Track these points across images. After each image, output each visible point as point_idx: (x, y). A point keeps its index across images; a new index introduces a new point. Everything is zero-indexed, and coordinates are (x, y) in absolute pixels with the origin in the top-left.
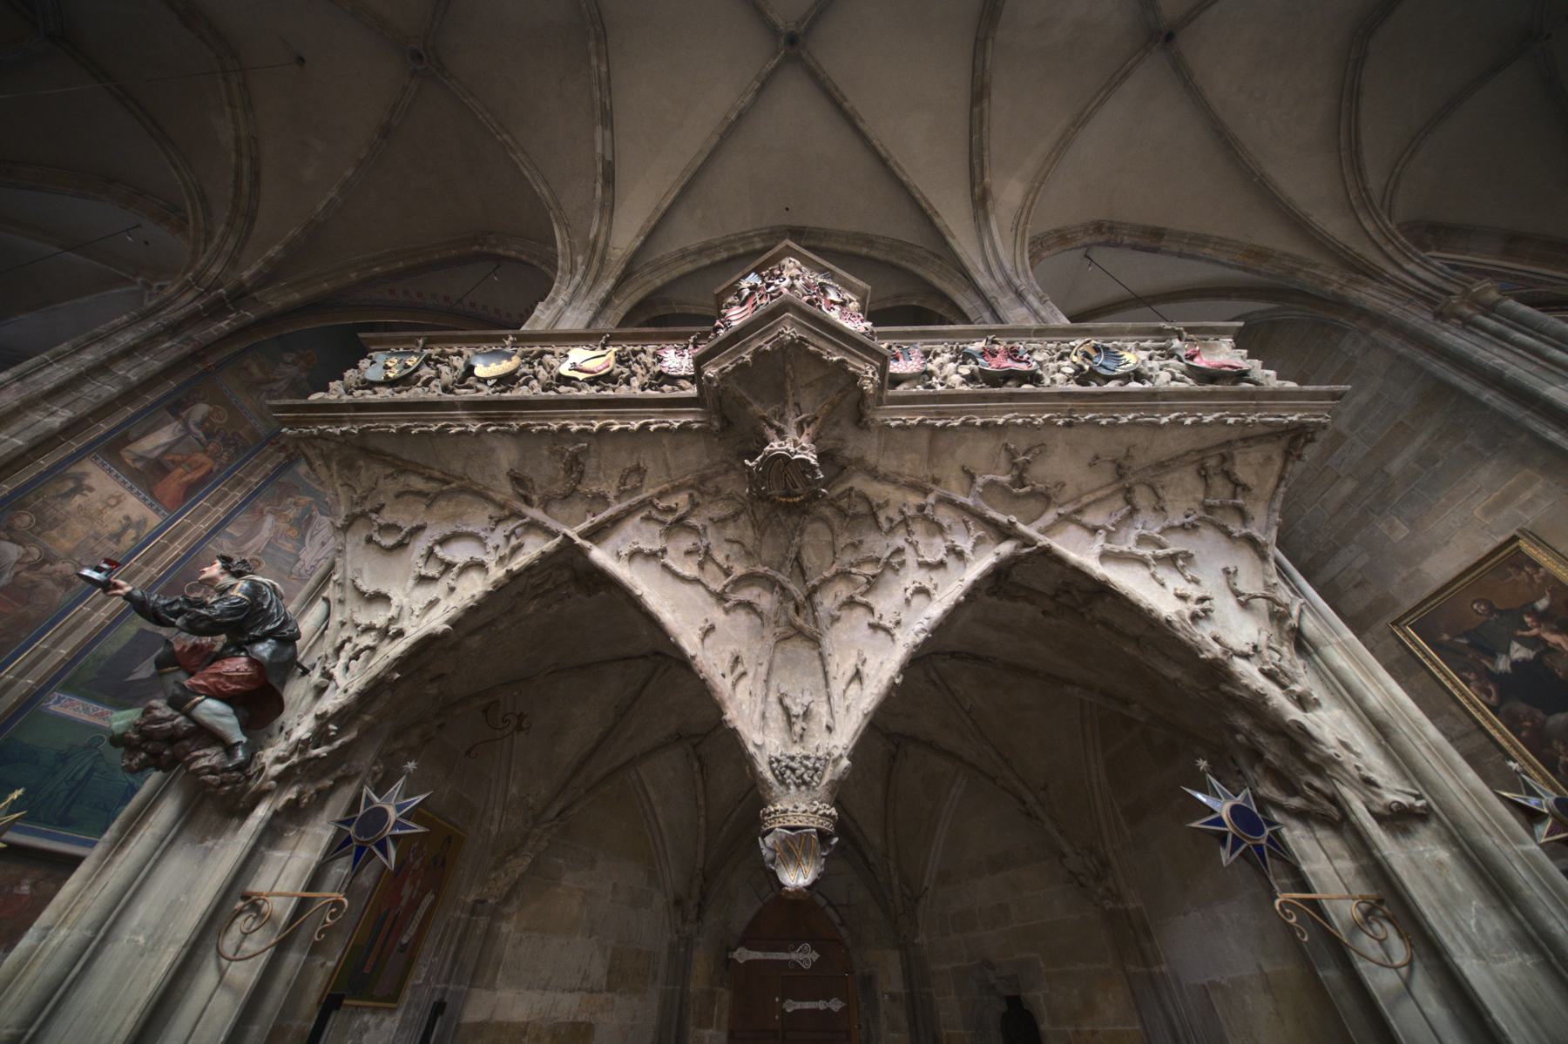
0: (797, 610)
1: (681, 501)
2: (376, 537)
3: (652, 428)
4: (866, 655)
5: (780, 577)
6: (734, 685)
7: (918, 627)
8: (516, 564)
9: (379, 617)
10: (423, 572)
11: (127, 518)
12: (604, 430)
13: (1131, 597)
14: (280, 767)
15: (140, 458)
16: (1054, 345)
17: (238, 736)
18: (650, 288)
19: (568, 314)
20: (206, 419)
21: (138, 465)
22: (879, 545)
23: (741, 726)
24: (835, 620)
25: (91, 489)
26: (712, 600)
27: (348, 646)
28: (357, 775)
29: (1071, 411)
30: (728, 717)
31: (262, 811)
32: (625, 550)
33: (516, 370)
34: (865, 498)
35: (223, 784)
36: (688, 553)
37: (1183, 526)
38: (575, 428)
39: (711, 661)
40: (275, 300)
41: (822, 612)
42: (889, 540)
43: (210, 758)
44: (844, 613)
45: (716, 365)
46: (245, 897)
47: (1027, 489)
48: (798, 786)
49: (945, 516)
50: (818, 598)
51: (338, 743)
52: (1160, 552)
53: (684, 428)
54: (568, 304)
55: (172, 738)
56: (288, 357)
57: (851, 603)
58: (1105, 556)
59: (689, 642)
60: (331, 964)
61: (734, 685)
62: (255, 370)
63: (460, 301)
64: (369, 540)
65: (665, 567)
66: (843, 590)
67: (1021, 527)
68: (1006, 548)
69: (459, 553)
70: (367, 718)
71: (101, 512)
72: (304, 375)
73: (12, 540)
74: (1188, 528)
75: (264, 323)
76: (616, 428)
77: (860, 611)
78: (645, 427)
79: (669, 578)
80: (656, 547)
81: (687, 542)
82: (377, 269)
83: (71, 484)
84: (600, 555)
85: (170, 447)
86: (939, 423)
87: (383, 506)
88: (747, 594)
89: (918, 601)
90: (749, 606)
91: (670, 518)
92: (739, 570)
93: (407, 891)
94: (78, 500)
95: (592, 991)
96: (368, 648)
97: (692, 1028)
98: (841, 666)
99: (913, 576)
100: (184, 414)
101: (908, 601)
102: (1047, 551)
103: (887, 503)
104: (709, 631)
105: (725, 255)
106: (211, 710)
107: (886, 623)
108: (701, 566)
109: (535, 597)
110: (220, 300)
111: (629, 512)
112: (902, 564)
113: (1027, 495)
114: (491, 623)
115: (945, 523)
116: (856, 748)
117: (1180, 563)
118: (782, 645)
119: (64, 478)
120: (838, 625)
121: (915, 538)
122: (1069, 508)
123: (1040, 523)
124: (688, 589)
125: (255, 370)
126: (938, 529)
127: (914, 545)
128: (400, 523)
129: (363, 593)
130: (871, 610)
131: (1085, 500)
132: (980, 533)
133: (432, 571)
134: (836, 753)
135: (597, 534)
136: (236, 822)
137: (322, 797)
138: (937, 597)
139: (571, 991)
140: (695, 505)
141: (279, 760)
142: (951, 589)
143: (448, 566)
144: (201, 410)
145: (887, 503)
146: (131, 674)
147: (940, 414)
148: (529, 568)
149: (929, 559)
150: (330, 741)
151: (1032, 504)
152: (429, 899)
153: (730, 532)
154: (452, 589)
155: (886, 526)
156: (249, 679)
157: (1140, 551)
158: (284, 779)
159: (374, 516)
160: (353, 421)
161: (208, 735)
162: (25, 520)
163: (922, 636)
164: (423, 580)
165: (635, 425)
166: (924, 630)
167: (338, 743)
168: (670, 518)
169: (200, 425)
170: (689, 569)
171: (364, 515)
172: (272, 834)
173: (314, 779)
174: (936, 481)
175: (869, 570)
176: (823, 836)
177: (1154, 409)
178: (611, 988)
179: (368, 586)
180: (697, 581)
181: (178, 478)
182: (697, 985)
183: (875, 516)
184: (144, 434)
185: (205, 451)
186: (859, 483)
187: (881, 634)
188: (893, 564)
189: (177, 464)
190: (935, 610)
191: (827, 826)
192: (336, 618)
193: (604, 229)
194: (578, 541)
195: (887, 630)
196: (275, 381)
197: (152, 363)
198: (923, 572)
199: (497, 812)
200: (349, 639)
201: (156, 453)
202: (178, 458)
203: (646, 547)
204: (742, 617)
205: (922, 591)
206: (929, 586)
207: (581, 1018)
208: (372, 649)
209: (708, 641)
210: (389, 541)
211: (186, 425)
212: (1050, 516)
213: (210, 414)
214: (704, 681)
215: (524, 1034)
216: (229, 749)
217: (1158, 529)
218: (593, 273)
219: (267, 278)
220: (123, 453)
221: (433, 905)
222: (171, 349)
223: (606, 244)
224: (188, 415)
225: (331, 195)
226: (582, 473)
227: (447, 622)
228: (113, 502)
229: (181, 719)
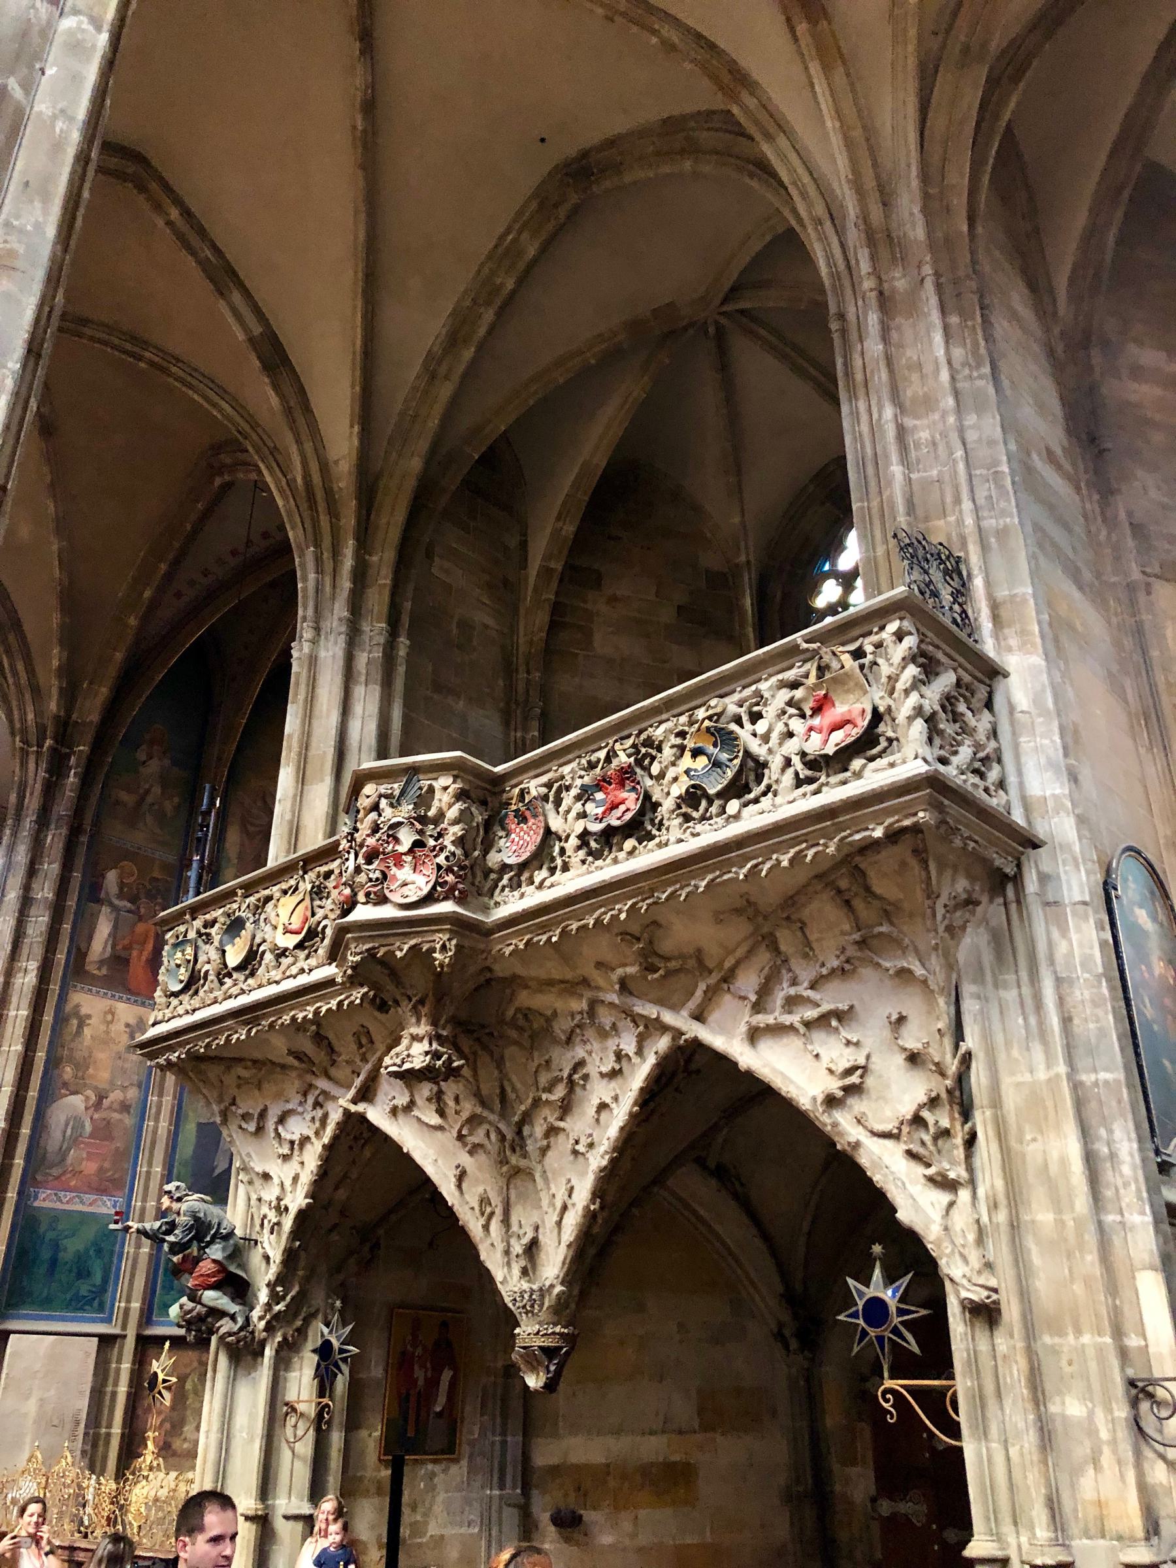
2: (244, 1126)
4: (573, 1182)
6: (486, 1227)
7: (602, 1149)
8: (326, 1140)
9: (270, 1193)
10: (281, 1151)
11: (127, 1025)
13: (773, 1085)
14: (262, 1324)
15: (102, 962)
16: (683, 719)
17: (233, 1308)
18: (411, 484)
19: (322, 654)
20: (121, 885)
21: (104, 971)
22: (564, 1061)
23: (489, 1265)
24: (544, 1151)
25: (89, 1017)
26: (458, 1144)
27: (266, 1222)
28: (317, 1311)
29: (652, 891)
30: (482, 1258)
31: (269, 1352)
33: (252, 945)
35: (238, 1341)
36: (429, 1100)
37: (833, 971)
38: (300, 1016)
39: (465, 1208)
40: (91, 710)
41: (530, 1147)
42: (569, 1055)
43: (225, 1326)
44: (552, 1139)
46: (287, 1404)
47: (661, 972)
50: (526, 1131)
51: (288, 1298)
52: (811, 1014)
54: (314, 642)
55: (201, 1319)
56: (141, 755)
57: (552, 1131)
58: (754, 1036)
59: (448, 1189)
60: (377, 1434)
61: (486, 1227)
62: (124, 796)
63: (249, 543)
64: (240, 1127)
65: (419, 1119)
66: (547, 1116)
67: (668, 1018)
68: (663, 1043)
69: (296, 1128)
70: (301, 1273)
71: (107, 1032)
72: (167, 762)
73: (72, 1093)
74: (842, 973)
75: (99, 744)
76: (324, 1009)
78: (340, 1004)
79: (425, 1128)
82: (147, 594)
83: (75, 1022)
85: (114, 934)
87: (234, 1099)
88: (478, 1137)
89: (604, 1115)
93: (419, 1374)
94: (87, 1031)
95: (680, 1432)
96: (275, 1224)
97: (836, 1467)
99: (600, 1091)
100: (102, 895)
101: (598, 1120)
102: (697, 1045)
104: (461, 1177)
105: (489, 315)
106: (210, 1297)
107: (580, 1148)
108: (441, 1113)
109: (363, 1146)
110: (53, 750)
112: (586, 1077)
113: (663, 977)
114: (345, 1176)
116: (567, 1274)
117: (834, 1023)
118: (513, 1181)
119: (66, 1020)
120: (550, 1153)
121: (588, 1047)
122: (713, 980)
123: (692, 1004)
124: (439, 1134)
125: (124, 796)
126: (603, 1035)
128: (251, 1111)
129: (258, 1174)
131: (727, 965)
133: (285, 1150)
134: (547, 1284)
135: (366, 1094)
136: (260, 1359)
137: (302, 1332)
138: (615, 1112)
139: (652, 1433)
141: (261, 1318)
143: (292, 1143)
144: (112, 876)
146: (214, 1169)
147: (544, 928)
148: (335, 1138)
149: (604, 1069)
150: (283, 1298)
151: (683, 979)
152: (447, 1375)
154: (302, 1163)
156: (219, 1272)
157: (787, 1019)
158: (269, 1328)
159: (233, 1108)
160: (181, 1045)
161: (217, 1313)
162: (68, 1072)
163: (607, 1157)
164: (286, 1158)
165: (333, 1004)
166: (606, 1152)
167: (288, 1298)
169: (121, 896)
171: (227, 1109)
172: (282, 1363)
173: (290, 1323)
175: (560, 1092)
177: (730, 863)
178: (706, 1427)
179: (259, 1169)
180: (440, 1128)
181: (139, 958)
182: (833, 1419)
184: (90, 938)
185: (140, 918)
186: (524, 999)
187: (581, 1158)
188: (575, 1081)
189: (128, 948)
192: (254, 1197)
193: (308, 446)
194: (353, 1108)
195: (583, 1154)
196: (147, 792)
197: (51, 868)
198: (605, 1080)
200: (265, 1216)
201: (109, 949)
202: (126, 942)
204: (482, 1157)
205: (603, 1106)
206: (608, 1100)
207: (676, 1458)
208: (278, 1224)
209: (464, 1186)
210: (252, 1127)
211: (111, 904)
213: (121, 877)
214: (462, 1228)
215: (608, 1474)
216: (233, 1317)
217: (806, 984)
218: (327, 542)
219: (70, 695)
220: (87, 968)
221: (453, 1384)
222: (54, 839)
223: (324, 468)
224: (107, 893)
225: (55, 547)
226: (330, 1043)
227: (306, 1197)
228: (109, 1017)
229: (199, 1306)
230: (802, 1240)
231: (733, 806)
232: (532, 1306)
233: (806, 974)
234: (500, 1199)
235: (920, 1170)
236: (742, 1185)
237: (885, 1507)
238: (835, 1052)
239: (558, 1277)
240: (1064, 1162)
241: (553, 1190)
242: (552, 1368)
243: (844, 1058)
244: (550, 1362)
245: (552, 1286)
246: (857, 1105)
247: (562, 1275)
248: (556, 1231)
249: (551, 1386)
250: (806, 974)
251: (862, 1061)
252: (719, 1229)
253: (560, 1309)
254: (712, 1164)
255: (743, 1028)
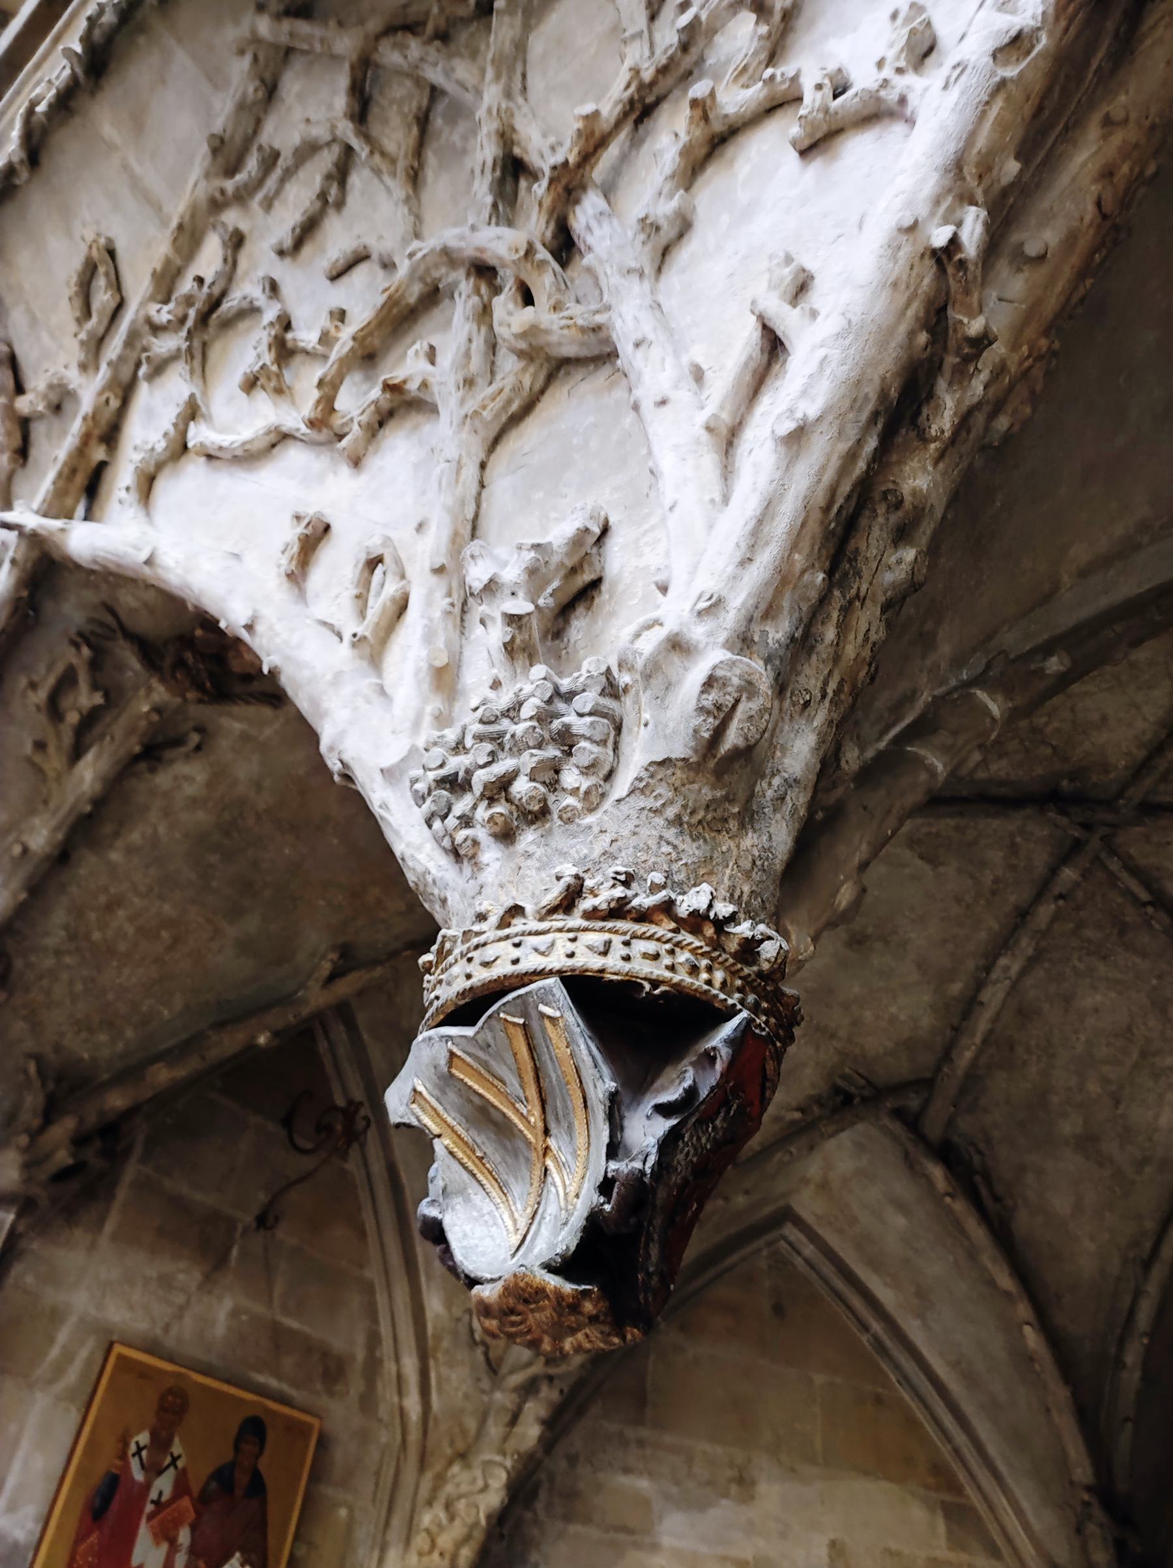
48: (506, 836)
176: (632, 1023)
191: (640, 958)
199: (410, 1365)
230: (1132, 1357)
232: (550, 775)
234: (449, 499)
236: (997, 1199)
239: (714, 607)
241: (698, 354)
242: (646, 1131)
244: (635, 1079)
245: (677, 645)
247: (739, 600)
248: (709, 461)
249: (624, 1253)
252: (913, 1329)
253: (721, 774)
254: (934, 1128)
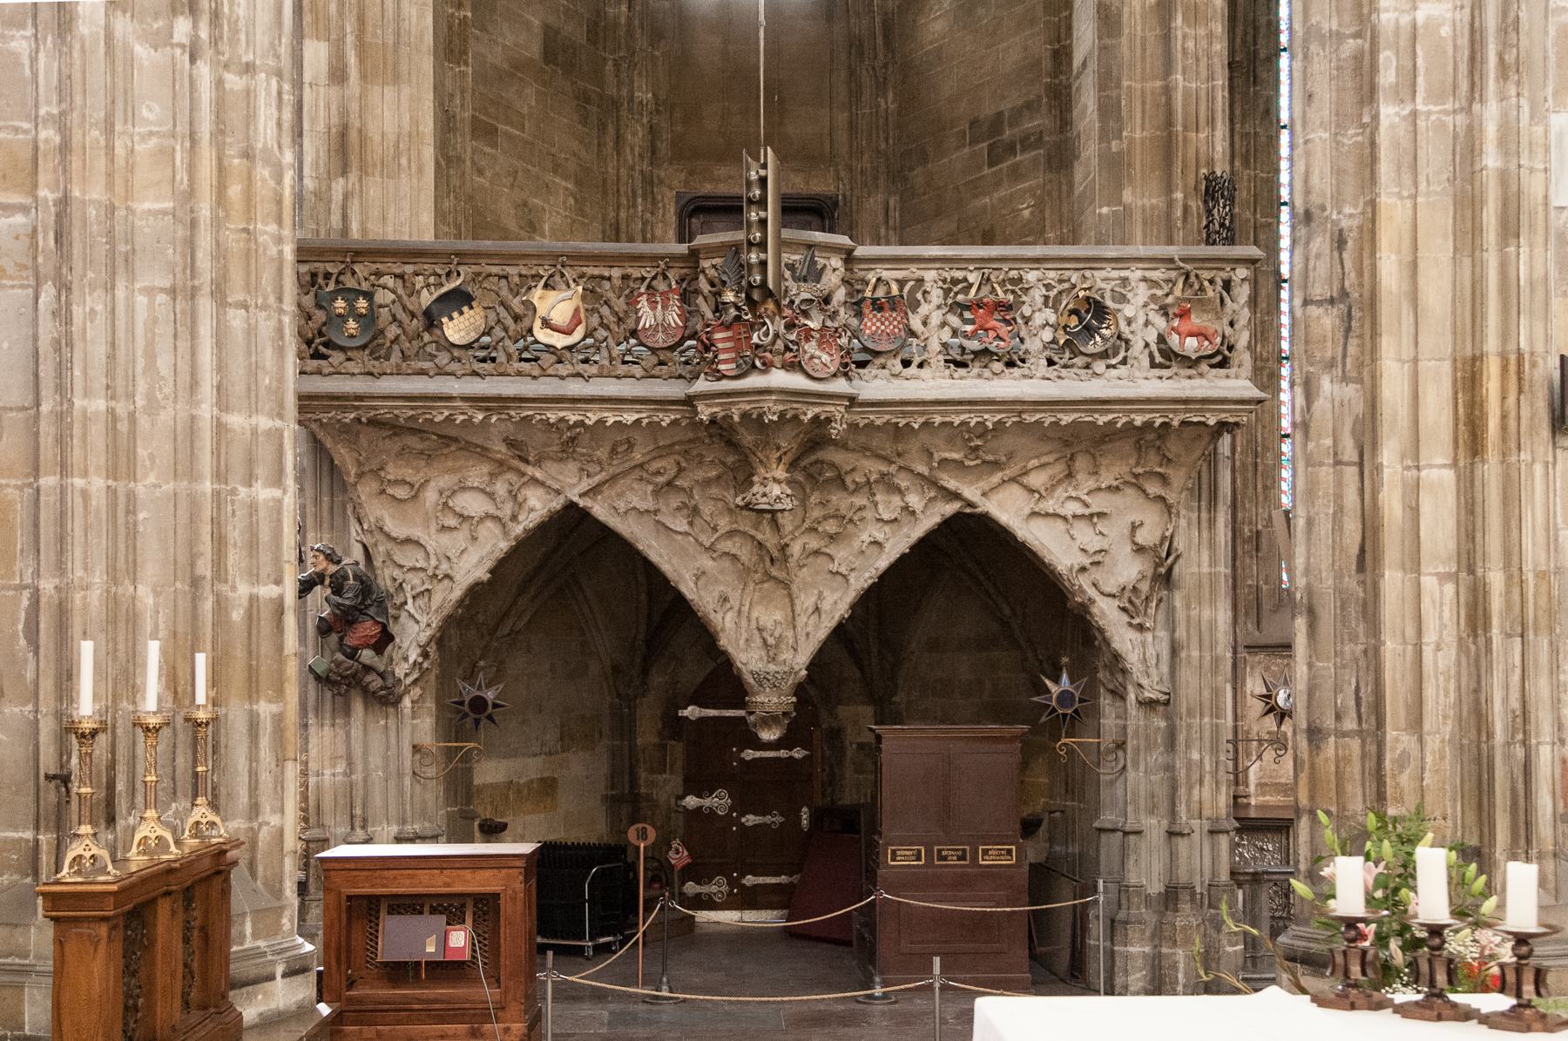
0: (772, 560)
1: (668, 465)
3: (645, 421)
5: (760, 537)
7: (867, 575)
12: (601, 422)
32: (622, 506)
34: (833, 465)
36: (678, 509)
41: (792, 563)
45: (708, 406)
49: (903, 481)
53: (674, 423)
76: (610, 421)
77: (821, 560)
80: (649, 504)
81: (675, 501)
84: (599, 510)
86: (902, 422)
90: (735, 557)
91: (661, 479)
92: (724, 524)
98: (806, 601)
103: (853, 470)
107: (843, 570)
111: (624, 474)
115: (903, 485)
121: (878, 498)
127: (876, 504)
130: (832, 558)
132: (932, 494)
140: (681, 470)
142: (898, 544)
145: (853, 470)
149: (886, 516)
153: (714, 491)
155: (852, 487)
168: (661, 479)
170: (681, 524)
174: (899, 455)
183: (843, 481)
187: (839, 578)
190: (883, 563)
194: (582, 503)
203: (643, 506)
204: (726, 563)
207: (546, 775)
212: (996, 478)
231: (1099, 366)
233: (1091, 483)
235: (1126, 618)
237: (691, 801)
238: (1086, 536)
240: (1213, 624)
243: (1095, 543)
246: (1095, 574)
250: (1091, 483)
251: (1106, 547)
255: (1027, 511)
